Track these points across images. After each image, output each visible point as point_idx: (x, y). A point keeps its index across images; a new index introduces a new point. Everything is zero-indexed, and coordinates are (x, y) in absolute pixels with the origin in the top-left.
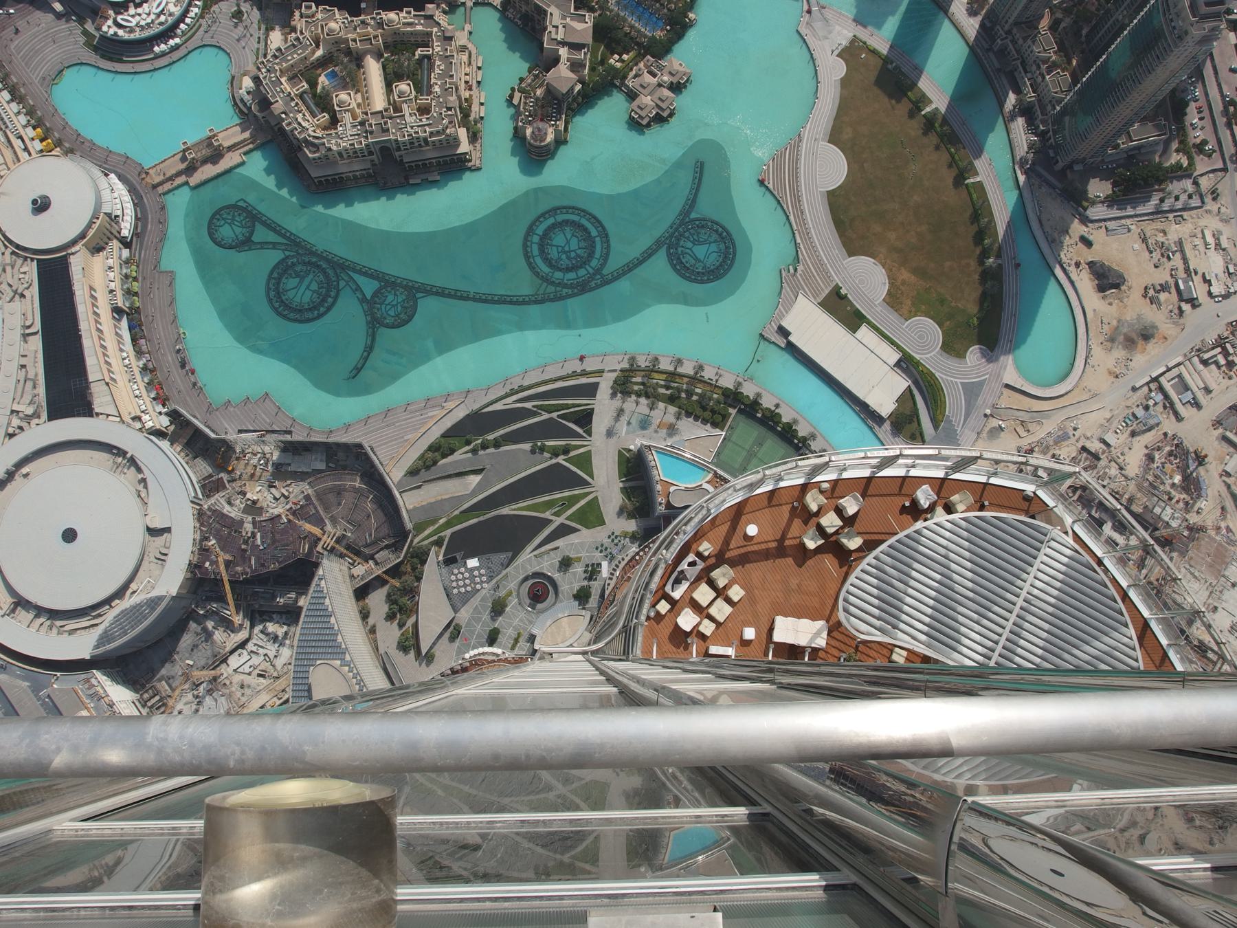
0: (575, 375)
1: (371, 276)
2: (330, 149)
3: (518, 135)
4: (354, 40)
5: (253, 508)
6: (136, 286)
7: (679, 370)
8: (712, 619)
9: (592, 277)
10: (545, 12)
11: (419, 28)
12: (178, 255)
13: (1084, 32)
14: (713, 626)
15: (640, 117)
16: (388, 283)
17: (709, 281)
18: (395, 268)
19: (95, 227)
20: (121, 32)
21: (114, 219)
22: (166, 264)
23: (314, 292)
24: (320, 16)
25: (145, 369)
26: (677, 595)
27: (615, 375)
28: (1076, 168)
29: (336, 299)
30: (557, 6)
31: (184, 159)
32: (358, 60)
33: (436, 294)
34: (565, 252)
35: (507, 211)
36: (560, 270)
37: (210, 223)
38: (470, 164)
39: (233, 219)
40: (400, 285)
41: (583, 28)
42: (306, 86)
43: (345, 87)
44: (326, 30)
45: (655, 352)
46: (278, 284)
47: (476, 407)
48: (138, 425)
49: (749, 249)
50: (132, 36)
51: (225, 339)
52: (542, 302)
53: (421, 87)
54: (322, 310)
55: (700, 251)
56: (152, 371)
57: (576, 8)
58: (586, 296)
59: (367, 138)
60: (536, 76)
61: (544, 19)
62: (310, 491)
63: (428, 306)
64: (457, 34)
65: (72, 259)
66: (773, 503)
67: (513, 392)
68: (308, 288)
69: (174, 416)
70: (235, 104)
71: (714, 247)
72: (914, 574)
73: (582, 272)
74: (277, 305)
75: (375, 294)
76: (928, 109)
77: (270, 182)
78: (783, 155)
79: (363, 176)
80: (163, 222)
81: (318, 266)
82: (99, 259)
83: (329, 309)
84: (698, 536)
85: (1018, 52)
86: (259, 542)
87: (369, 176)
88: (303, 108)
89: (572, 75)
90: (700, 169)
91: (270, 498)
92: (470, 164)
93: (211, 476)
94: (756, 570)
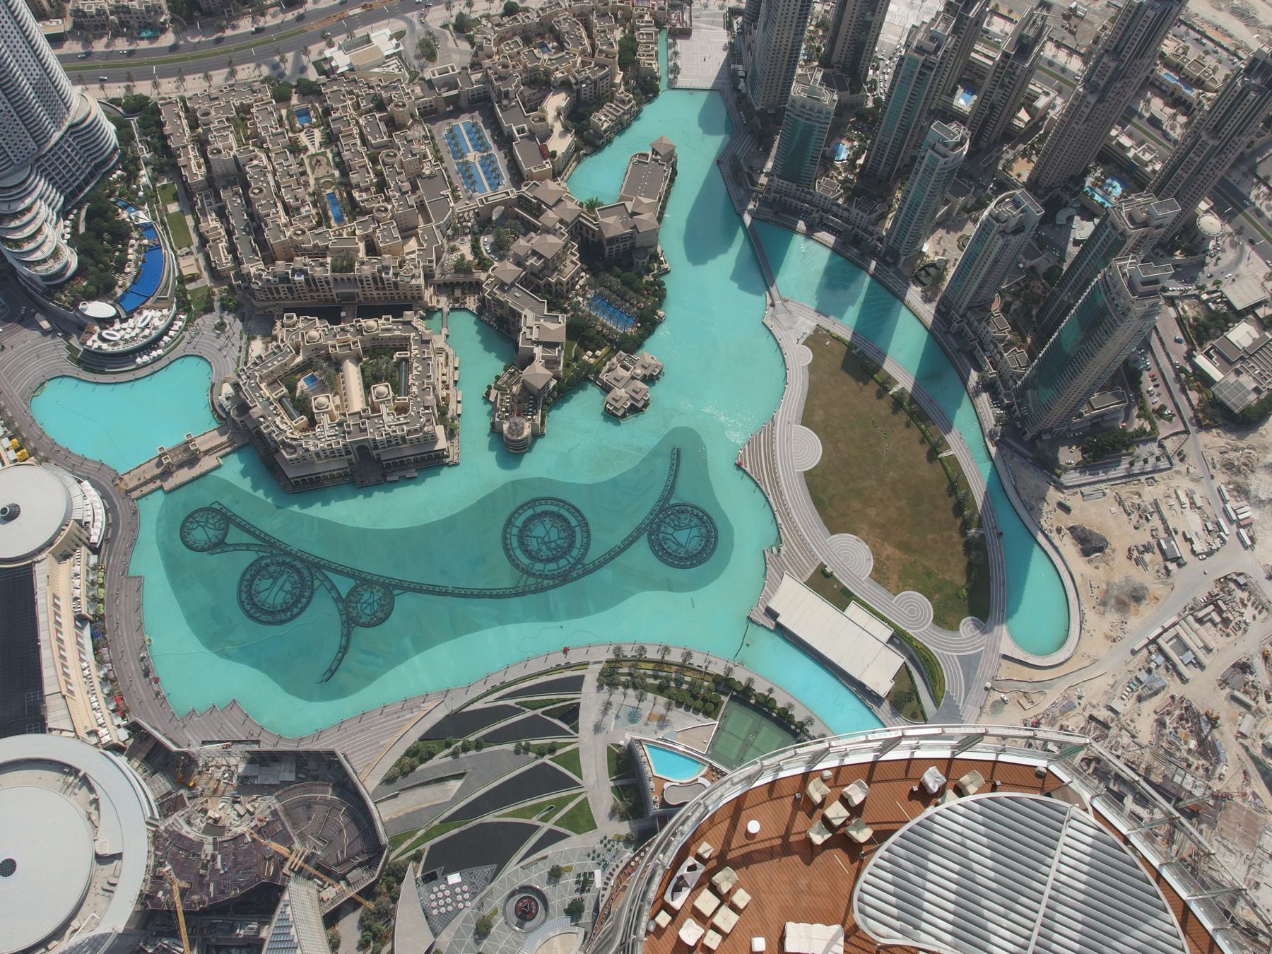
1: (347, 575)
2: (307, 450)
3: (495, 430)
4: (334, 347)
5: (215, 827)
6: (102, 593)
7: (666, 658)
8: (717, 929)
9: (573, 567)
10: (520, 315)
11: (397, 333)
12: (148, 561)
13: (1034, 312)
14: (718, 938)
15: (615, 408)
16: (364, 581)
17: (692, 566)
18: (368, 566)
19: (64, 534)
20: (105, 346)
21: (83, 525)
22: (134, 570)
23: (287, 592)
24: (300, 325)
25: (105, 679)
26: (677, 904)
27: (600, 666)
28: (1045, 437)
29: (310, 599)
31: (159, 464)
32: (337, 365)
33: (414, 590)
34: (545, 543)
35: (484, 505)
36: (541, 561)
37: (183, 526)
38: (447, 460)
39: (207, 522)
40: (377, 583)
41: (557, 327)
42: (286, 391)
43: (323, 391)
44: (306, 338)
45: (641, 640)
46: (251, 585)
47: (456, 706)
48: (94, 740)
49: (731, 533)
50: (116, 349)
51: (193, 645)
52: (523, 594)
53: (399, 388)
54: (295, 611)
55: (682, 536)
56: (112, 681)
57: (549, 310)
58: (568, 587)
60: (512, 374)
61: (519, 321)
62: (278, 806)
63: (405, 603)
64: (435, 337)
65: (37, 568)
66: (774, 796)
68: (281, 588)
69: (134, 728)
70: (214, 409)
71: (695, 532)
72: (931, 865)
73: (563, 562)
74: (248, 607)
75: (351, 593)
76: (895, 389)
77: (246, 484)
79: (340, 476)
80: (134, 530)
81: (293, 567)
82: (65, 568)
83: (302, 610)
84: (697, 836)
85: (975, 333)
86: (219, 865)
87: (346, 475)
88: (282, 411)
90: (677, 456)
91: (233, 815)
92: (447, 460)
93: (169, 793)
94: (762, 871)
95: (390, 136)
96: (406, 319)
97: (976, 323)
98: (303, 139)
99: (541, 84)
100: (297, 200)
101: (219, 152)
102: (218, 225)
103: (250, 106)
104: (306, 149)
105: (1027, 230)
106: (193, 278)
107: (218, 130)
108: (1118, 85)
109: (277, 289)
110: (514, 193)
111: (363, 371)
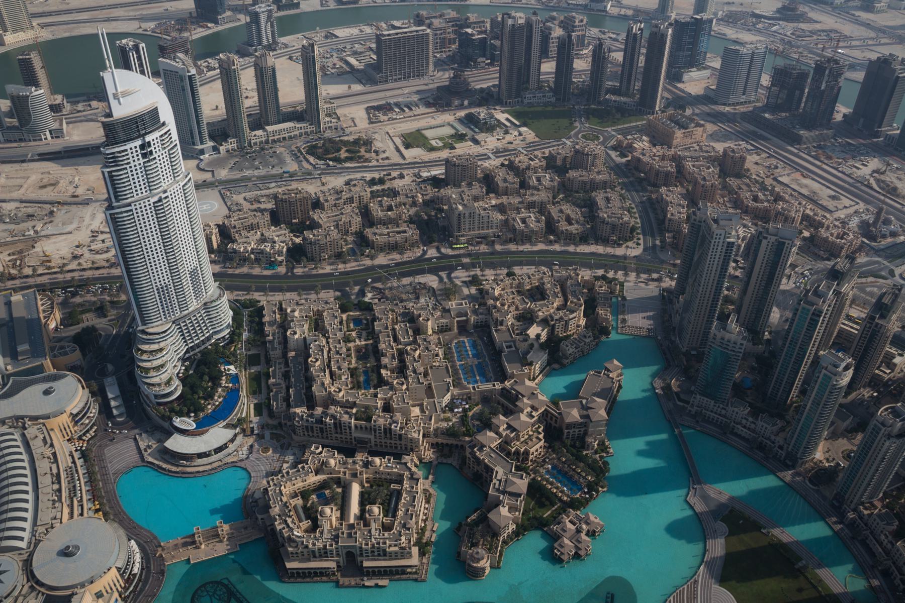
2: (307, 547)
10: (492, 470)
30: (502, 467)
38: (415, 576)
41: (521, 484)
53: (390, 510)
59: (337, 543)
76: (800, 564)
78: (681, 593)
85: (866, 525)
89: (509, 515)
95: (415, 338)
96: (403, 461)
99: (527, 318)
100: (339, 368)
101: (295, 333)
102: (282, 382)
103: (323, 311)
104: (355, 341)
107: (298, 321)
109: (312, 428)
110: (498, 386)
111: (362, 494)
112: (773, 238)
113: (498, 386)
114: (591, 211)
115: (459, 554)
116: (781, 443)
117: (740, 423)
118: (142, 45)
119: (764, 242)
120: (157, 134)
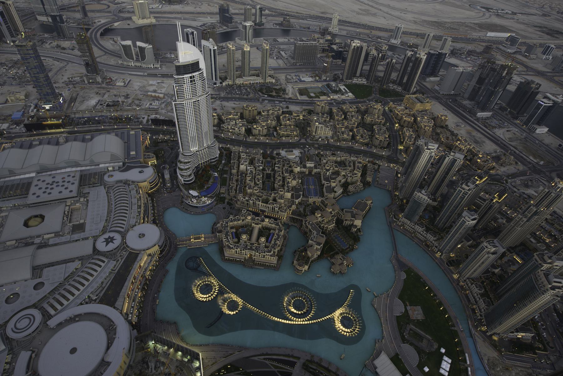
0: (288, 356)
12: (172, 268)
41: (323, 240)
67: (263, 355)
97: (470, 284)
98: (267, 169)
105: (498, 255)
106: (223, 193)
108: (536, 217)
112: (452, 157)
113: (320, 200)
114: (372, 133)
115: (293, 262)
116: (437, 245)
117: (419, 233)
118: (195, 32)
119: (447, 158)
120: (197, 73)
